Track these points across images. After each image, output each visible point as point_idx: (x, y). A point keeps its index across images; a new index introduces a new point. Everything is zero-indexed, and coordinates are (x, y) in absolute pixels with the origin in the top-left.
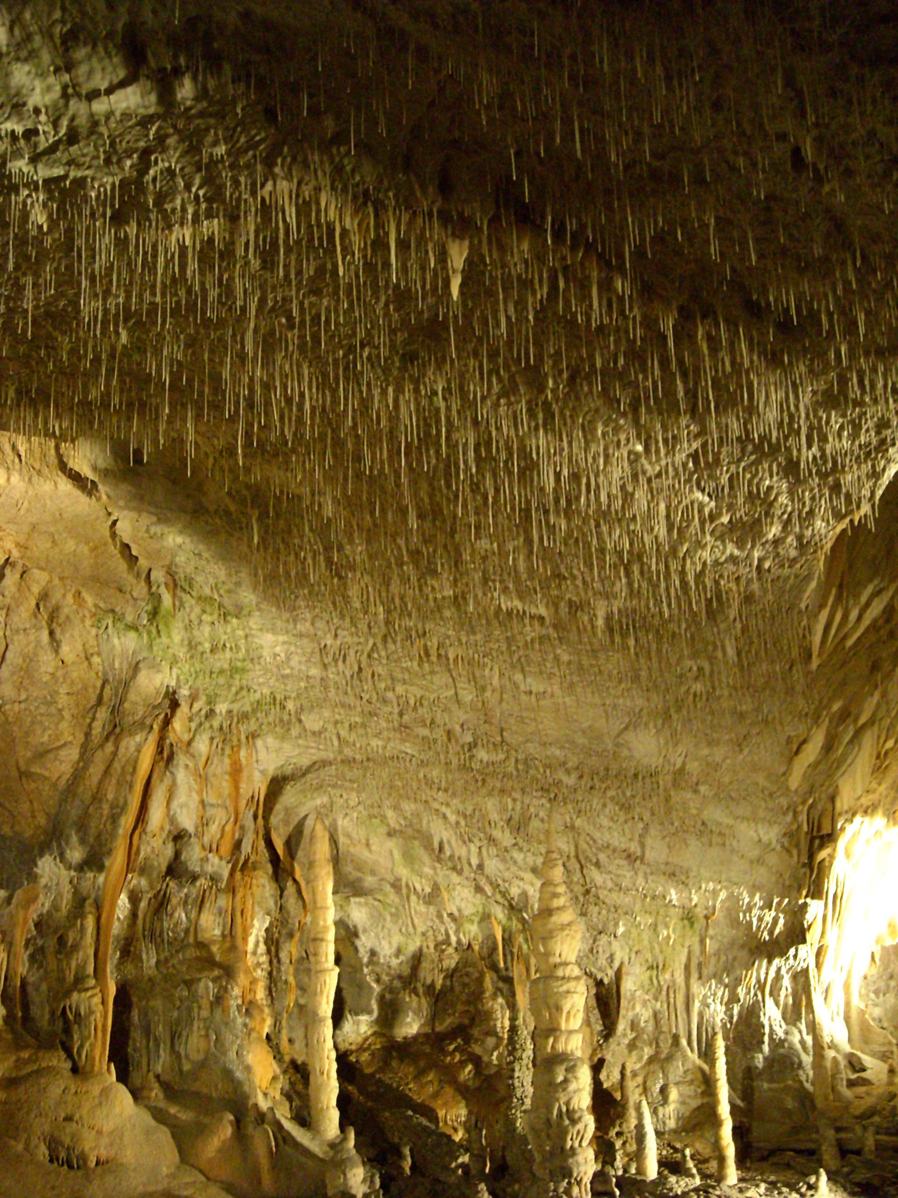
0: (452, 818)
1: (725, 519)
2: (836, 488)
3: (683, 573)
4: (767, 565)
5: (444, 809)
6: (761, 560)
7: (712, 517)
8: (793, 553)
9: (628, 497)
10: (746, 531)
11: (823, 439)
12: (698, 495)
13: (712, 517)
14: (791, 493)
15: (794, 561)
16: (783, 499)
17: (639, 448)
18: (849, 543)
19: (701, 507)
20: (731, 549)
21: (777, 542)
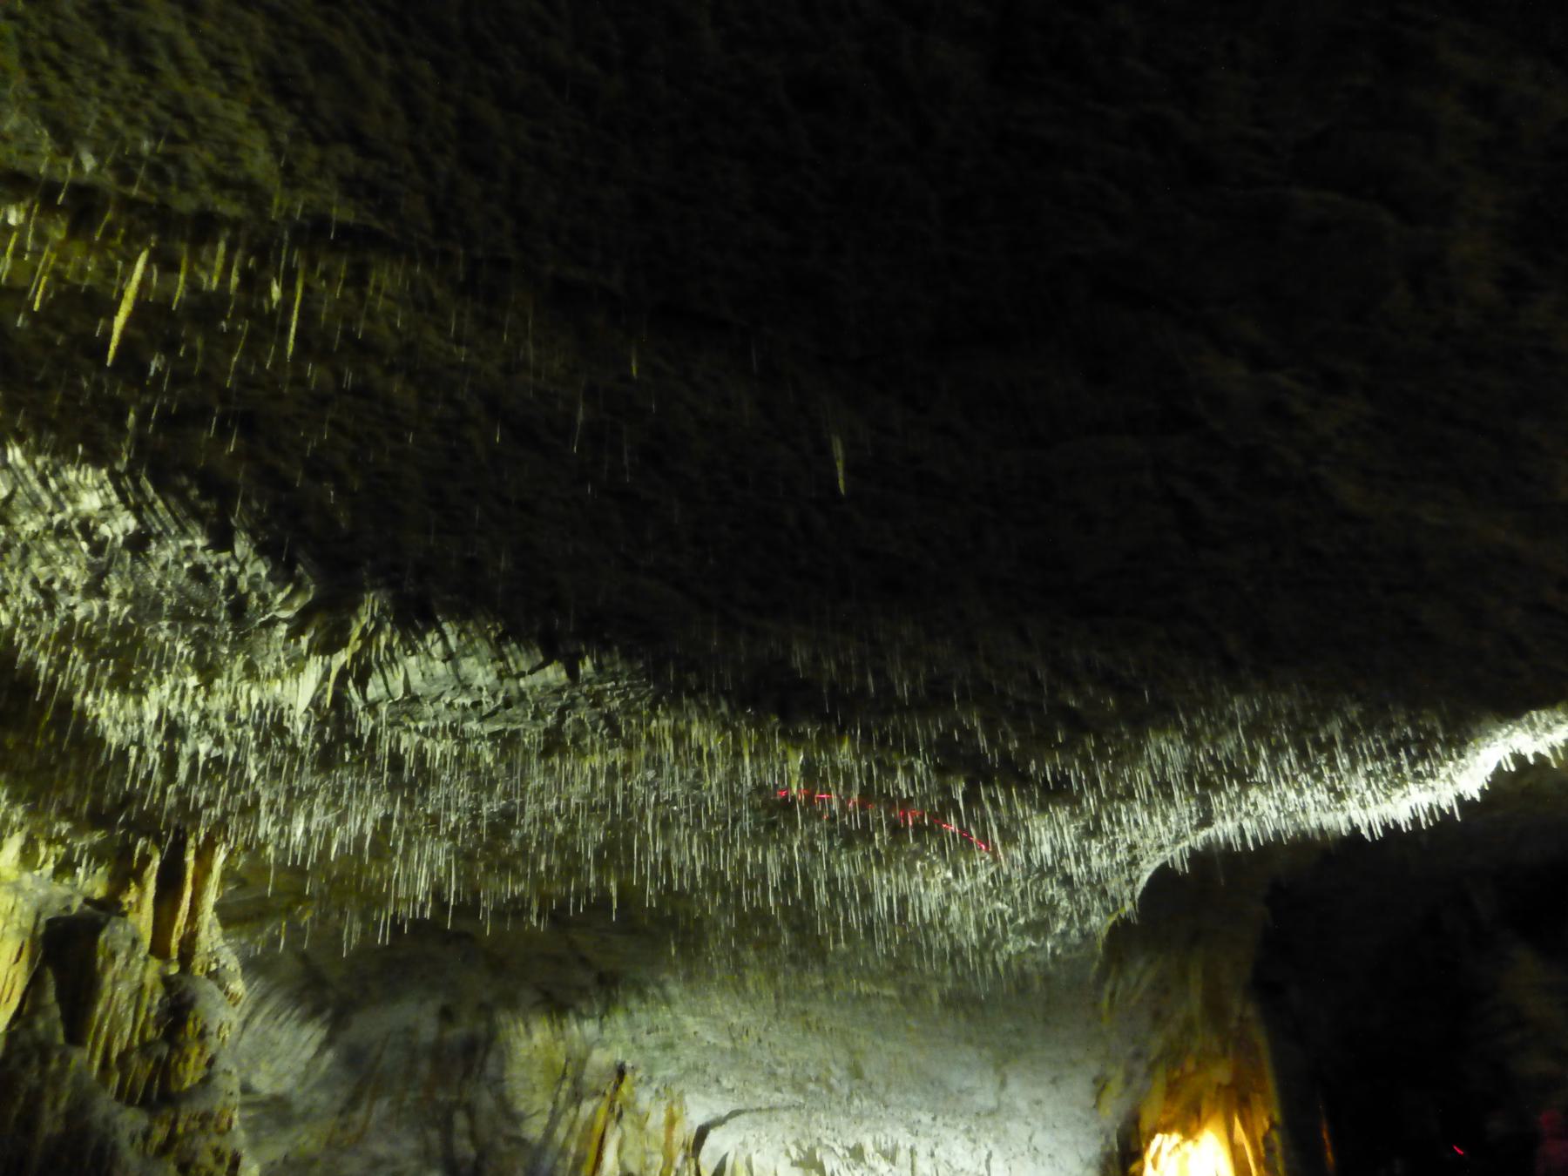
0: (840, 1152)
1: (1021, 921)
2: (1104, 892)
3: (994, 963)
4: (1058, 952)
5: (832, 1144)
6: (1053, 949)
7: (1013, 920)
8: (1077, 941)
9: (945, 911)
10: (1038, 928)
11: (1088, 859)
12: (999, 905)
13: (1013, 920)
14: (1070, 897)
15: (1078, 948)
16: (1064, 903)
17: (950, 874)
18: (1121, 931)
19: (1002, 914)
20: (1030, 942)
21: (1064, 934)
